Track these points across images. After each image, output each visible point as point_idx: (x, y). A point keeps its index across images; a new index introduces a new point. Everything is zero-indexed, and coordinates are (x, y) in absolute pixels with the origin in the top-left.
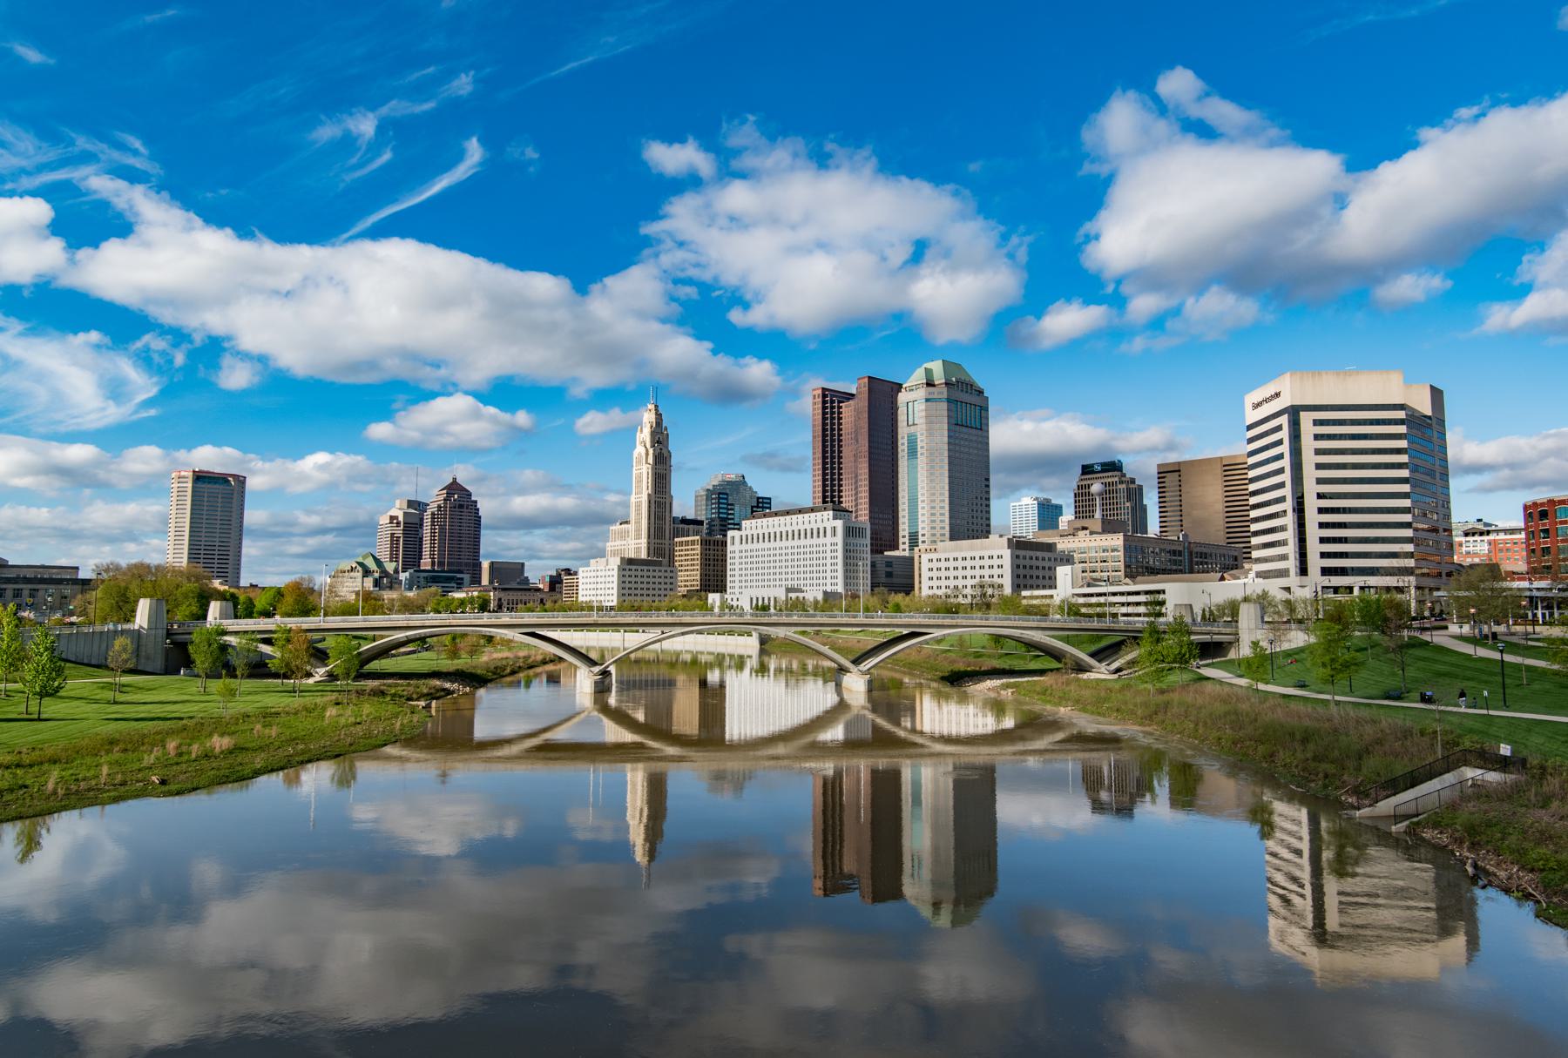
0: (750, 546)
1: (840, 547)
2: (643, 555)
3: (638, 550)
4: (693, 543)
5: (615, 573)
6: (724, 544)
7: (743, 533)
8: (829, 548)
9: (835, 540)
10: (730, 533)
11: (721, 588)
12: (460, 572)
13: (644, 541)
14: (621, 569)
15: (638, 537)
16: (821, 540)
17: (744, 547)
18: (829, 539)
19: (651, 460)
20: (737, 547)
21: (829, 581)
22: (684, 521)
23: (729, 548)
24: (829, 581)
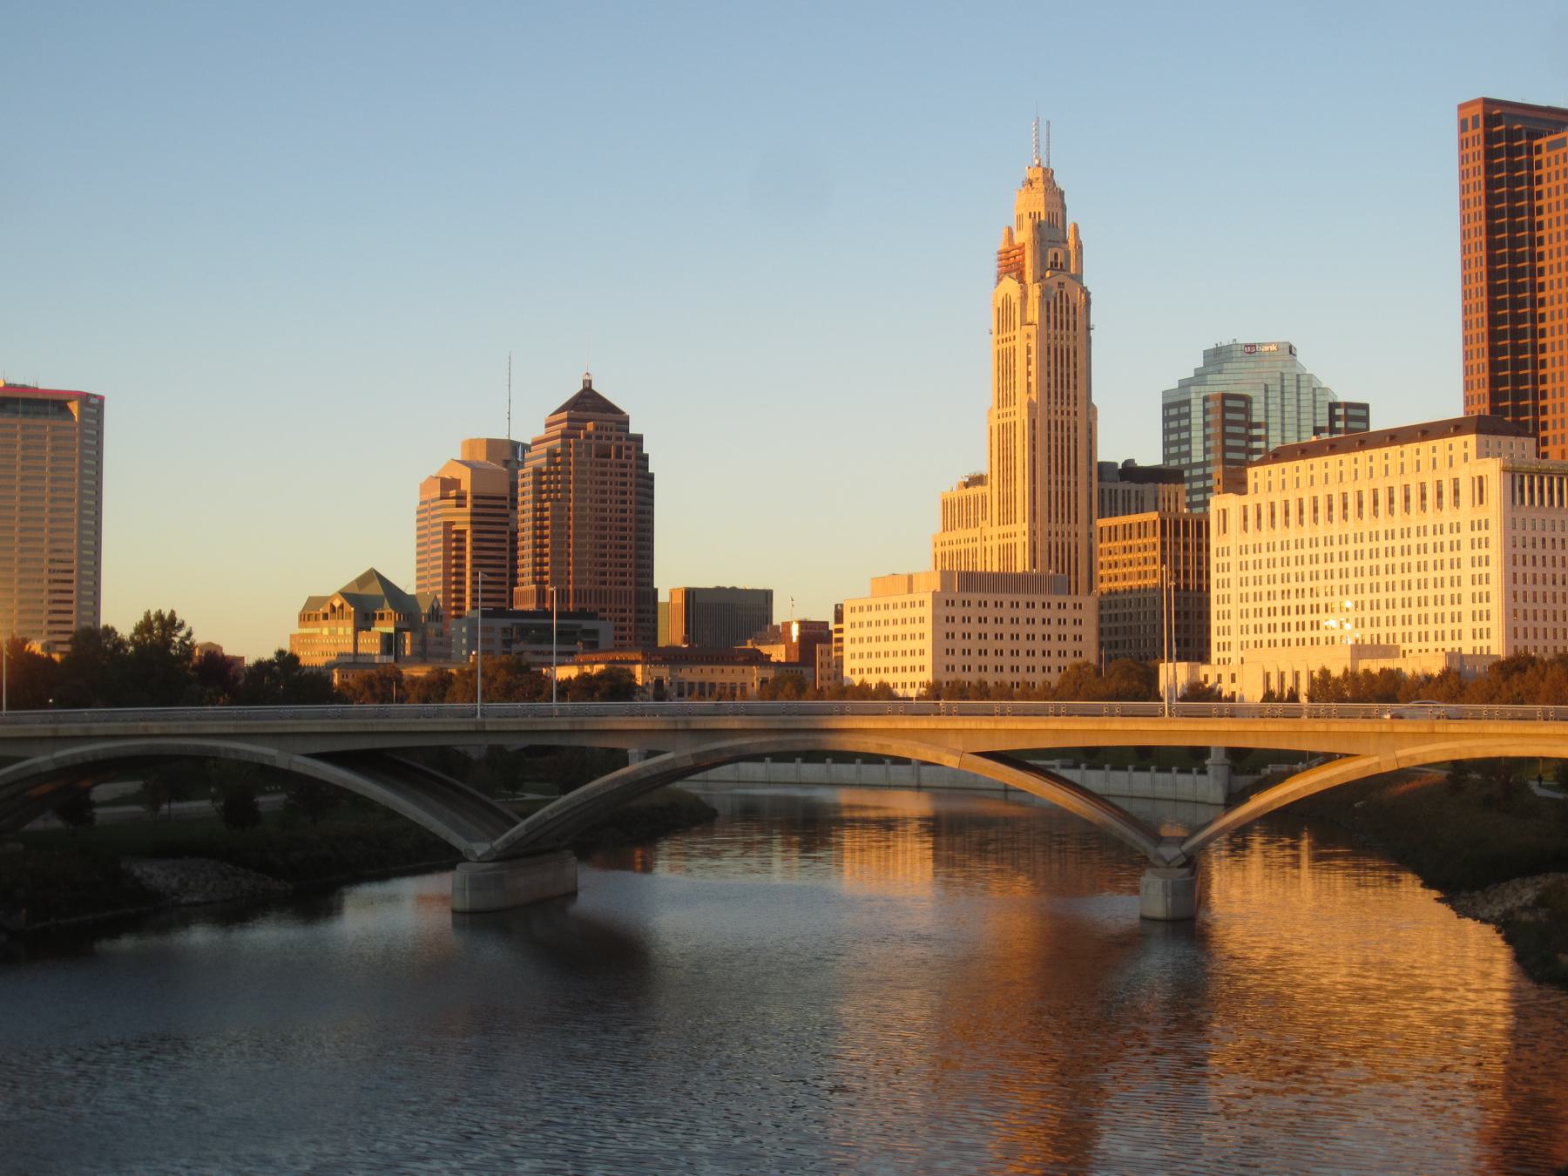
0: (1265, 536)
1: (1495, 534)
2: (1021, 565)
3: (1007, 552)
4: (1142, 529)
5: (927, 612)
6: (1202, 528)
7: (1249, 500)
8: (1466, 535)
9: (1481, 514)
10: (1217, 502)
11: (1195, 647)
12: (593, 616)
13: (1021, 527)
14: (943, 601)
15: (1007, 517)
16: (1448, 516)
17: (1251, 538)
18: (1466, 512)
19: (1034, 314)
20: (1234, 538)
21: (1467, 625)
22: (1130, 472)
23: (1215, 542)
24: (1467, 625)
